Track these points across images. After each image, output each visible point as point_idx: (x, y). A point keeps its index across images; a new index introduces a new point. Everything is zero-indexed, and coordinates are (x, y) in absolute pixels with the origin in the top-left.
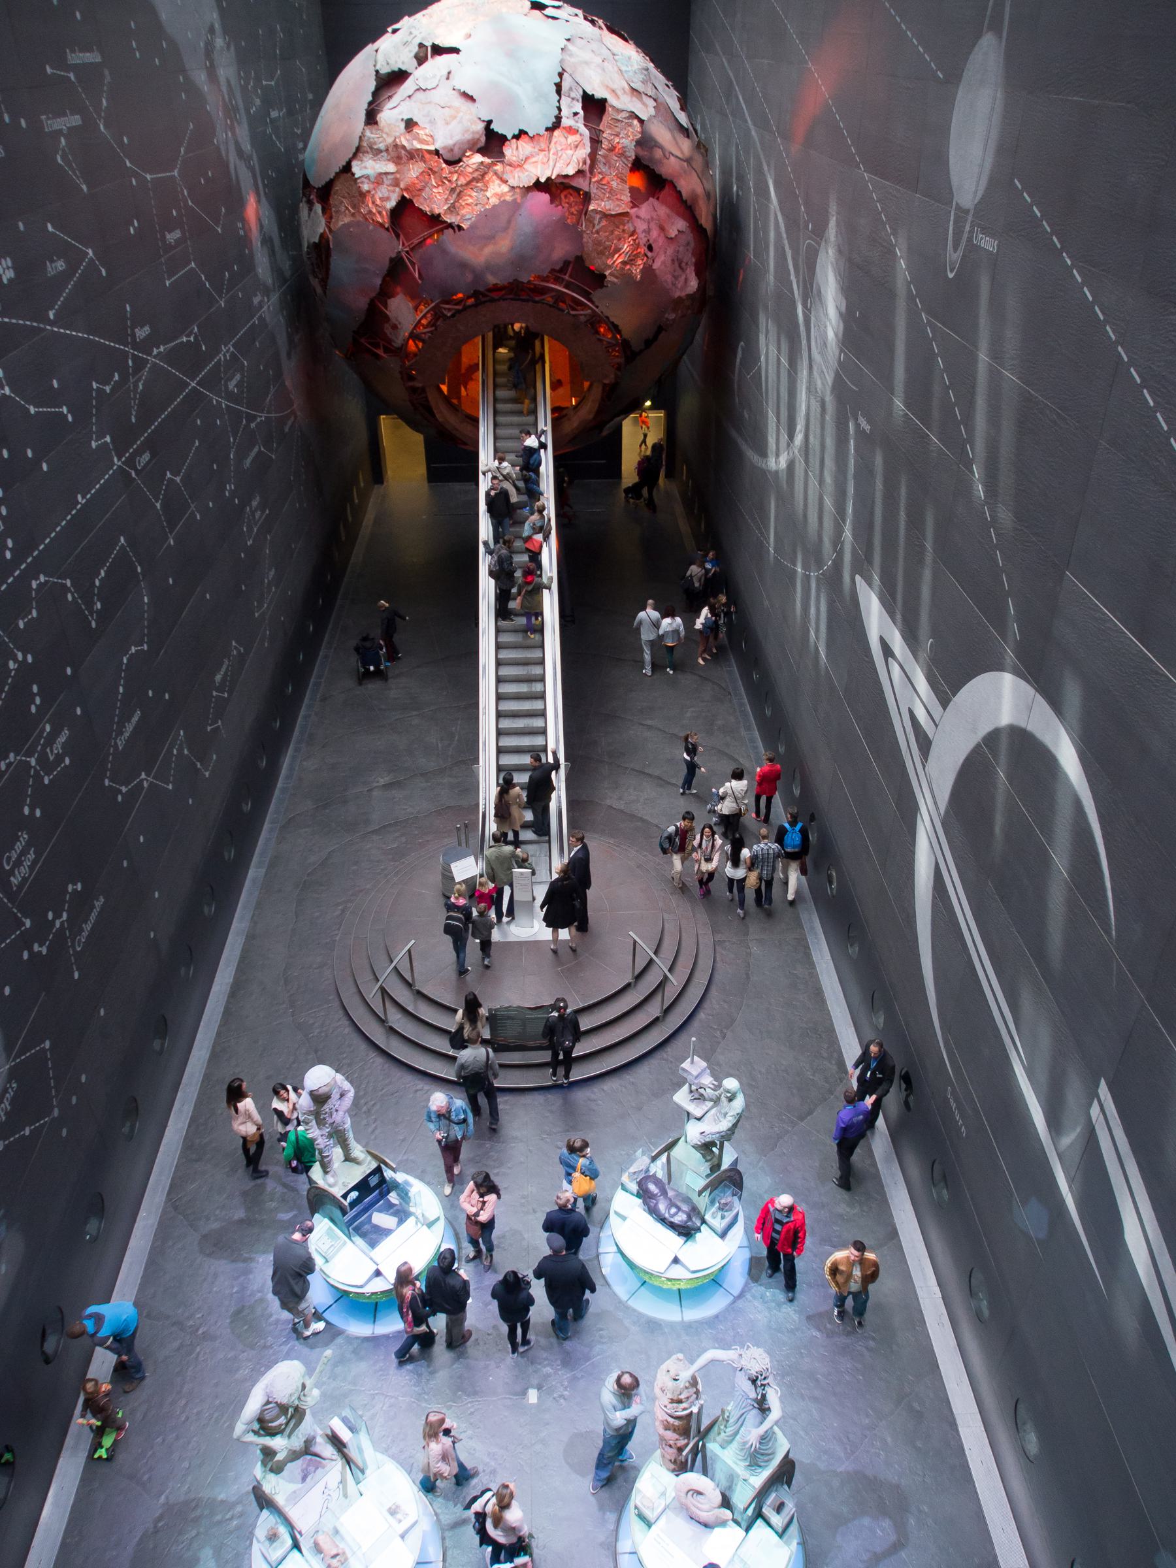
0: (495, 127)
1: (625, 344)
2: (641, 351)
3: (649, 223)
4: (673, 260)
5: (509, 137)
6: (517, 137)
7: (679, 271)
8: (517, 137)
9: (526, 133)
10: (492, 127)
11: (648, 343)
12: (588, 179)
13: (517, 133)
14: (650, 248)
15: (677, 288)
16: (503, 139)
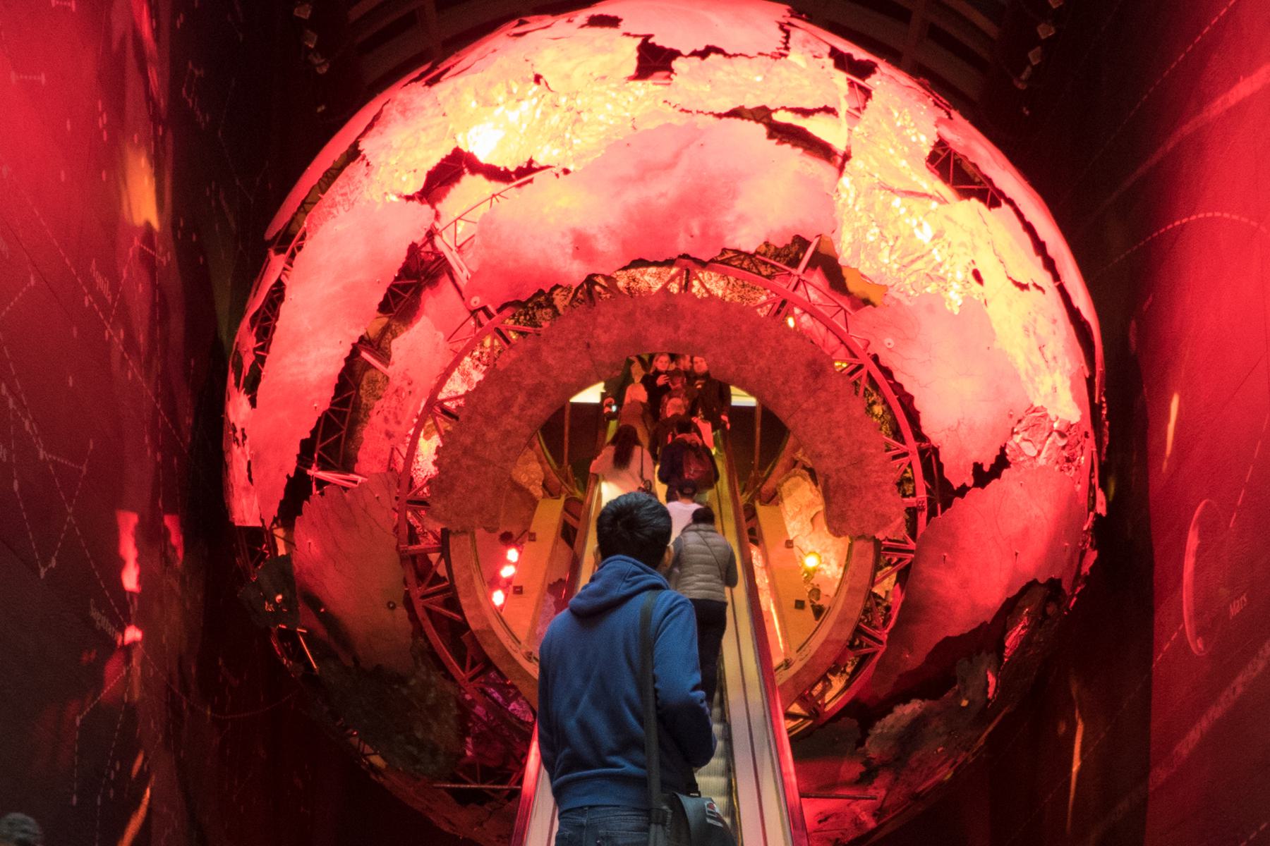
0: (658, 41)
1: (930, 456)
2: (963, 490)
3: (972, 235)
4: (1026, 330)
5: (686, 52)
6: (703, 54)
7: (1037, 358)
8: (703, 54)
9: (719, 51)
10: (651, 41)
11: (983, 476)
12: (844, 134)
13: (701, 48)
14: (977, 275)
15: (1037, 390)
16: (675, 54)
